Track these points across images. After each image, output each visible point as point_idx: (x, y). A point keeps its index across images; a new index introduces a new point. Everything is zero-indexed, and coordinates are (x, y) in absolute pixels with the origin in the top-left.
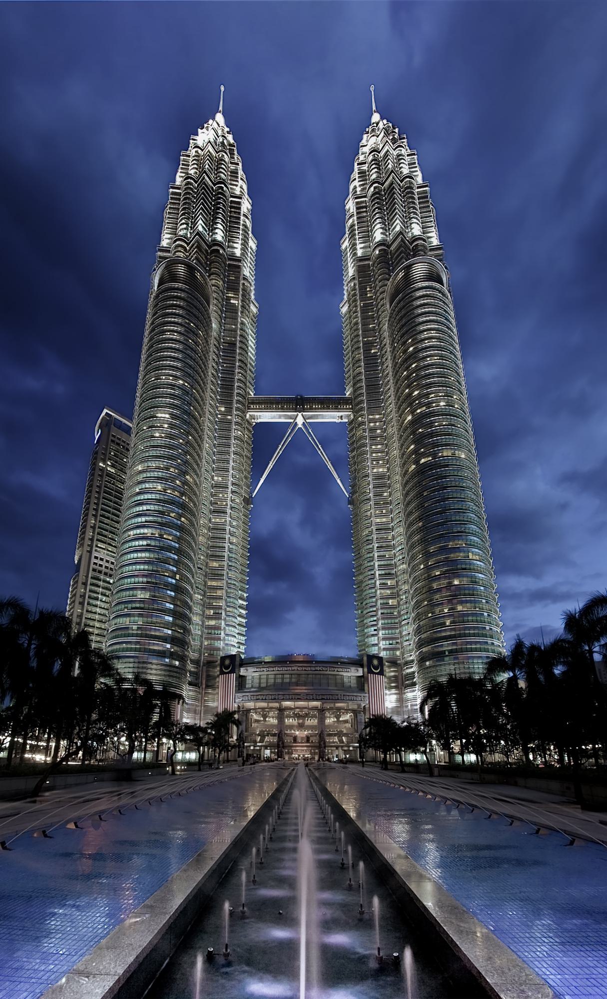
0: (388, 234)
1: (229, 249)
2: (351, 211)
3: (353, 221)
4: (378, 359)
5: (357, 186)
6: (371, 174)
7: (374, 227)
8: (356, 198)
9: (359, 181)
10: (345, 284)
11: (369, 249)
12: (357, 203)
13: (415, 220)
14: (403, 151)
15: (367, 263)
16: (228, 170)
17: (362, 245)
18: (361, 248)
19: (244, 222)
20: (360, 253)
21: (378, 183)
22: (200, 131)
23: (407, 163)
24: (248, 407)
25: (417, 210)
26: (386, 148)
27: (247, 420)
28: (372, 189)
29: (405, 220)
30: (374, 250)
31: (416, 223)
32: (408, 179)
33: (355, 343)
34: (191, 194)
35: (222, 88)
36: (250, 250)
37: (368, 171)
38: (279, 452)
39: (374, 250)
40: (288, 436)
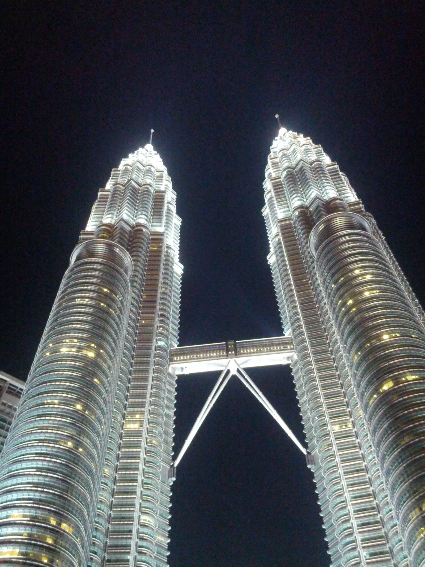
0: (305, 200)
1: (152, 228)
3: (271, 195)
4: (315, 304)
5: (272, 172)
6: (283, 163)
8: (271, 180)
11: (289, 212)
12: (273, 183)
14: (309, 147)
15: (288, 222)
16: (154, 177)
19: (168, 207)
23: (314, 153)
24: (169, 359)
25: (330, 181)
26: (294, 147)
27: (169, 374)
29: (320, 189)
30: (293, 212)
32: (317, 163)
33: (287, 286)
34: (119, 194)
36: (173, 225)
37: (280, 162)
39: (293, 212)
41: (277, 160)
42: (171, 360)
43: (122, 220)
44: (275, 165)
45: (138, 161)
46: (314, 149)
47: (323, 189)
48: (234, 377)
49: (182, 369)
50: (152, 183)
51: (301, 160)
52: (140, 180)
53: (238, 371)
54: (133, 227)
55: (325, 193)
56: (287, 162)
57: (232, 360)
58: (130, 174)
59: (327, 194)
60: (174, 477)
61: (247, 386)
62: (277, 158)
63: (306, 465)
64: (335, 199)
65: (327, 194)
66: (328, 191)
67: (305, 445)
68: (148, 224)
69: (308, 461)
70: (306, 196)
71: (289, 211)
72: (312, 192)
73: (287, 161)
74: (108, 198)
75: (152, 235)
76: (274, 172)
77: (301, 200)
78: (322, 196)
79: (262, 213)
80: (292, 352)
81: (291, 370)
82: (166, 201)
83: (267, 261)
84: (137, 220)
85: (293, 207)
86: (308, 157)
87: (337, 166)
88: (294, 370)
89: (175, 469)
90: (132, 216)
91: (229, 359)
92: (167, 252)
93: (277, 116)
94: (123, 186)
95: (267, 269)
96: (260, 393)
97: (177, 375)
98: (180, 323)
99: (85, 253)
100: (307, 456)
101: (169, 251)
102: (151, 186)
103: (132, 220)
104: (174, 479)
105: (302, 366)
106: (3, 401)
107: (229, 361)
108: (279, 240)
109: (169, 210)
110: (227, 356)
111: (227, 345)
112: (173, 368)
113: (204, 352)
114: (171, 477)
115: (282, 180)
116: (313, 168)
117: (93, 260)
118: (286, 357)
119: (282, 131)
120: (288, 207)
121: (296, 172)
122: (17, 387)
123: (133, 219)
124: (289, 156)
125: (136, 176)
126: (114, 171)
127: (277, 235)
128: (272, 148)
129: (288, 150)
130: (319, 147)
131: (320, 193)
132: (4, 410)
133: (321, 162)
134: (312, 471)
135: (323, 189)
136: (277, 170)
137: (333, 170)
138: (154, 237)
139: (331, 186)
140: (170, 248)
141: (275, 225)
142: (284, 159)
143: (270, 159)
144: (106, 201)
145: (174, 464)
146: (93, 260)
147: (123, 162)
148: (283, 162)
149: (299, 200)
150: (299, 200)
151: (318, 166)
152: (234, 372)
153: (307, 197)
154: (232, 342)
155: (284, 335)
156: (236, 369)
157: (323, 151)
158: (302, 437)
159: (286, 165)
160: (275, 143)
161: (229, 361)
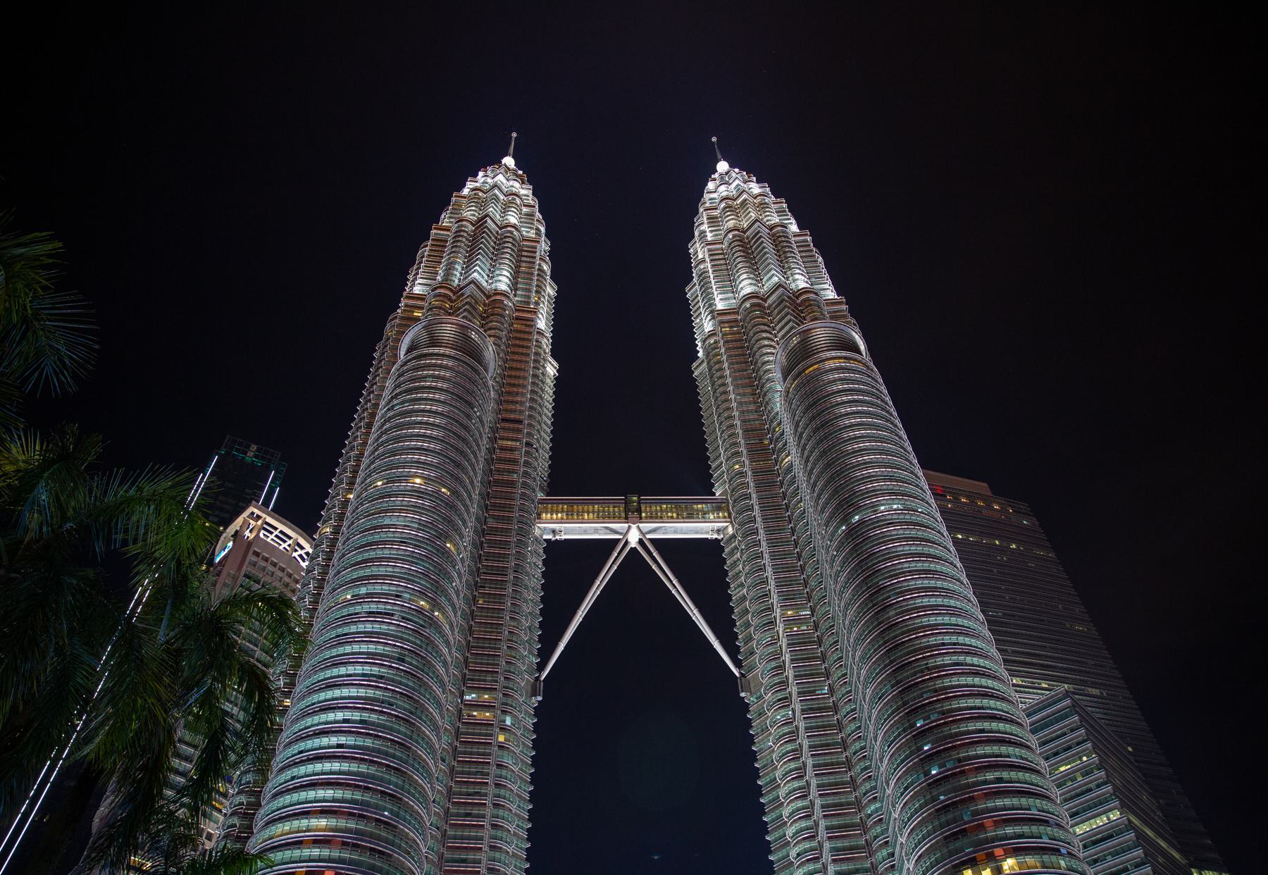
2: (700, 256)
7: (739, 277)
9: (709, 227)
10: (699, 344)
12: (709, 250)
13: (798, 271)
14: (767, 200)
17: (720, 297)
18: (721, 299)
20: (720, 306)
21: (738, 230)
22: (481, 174)
27: (536, 539)
28: (730, 236)
31: (799, 273)
35: (514, 135)
38: (595, 592)
40: (613, 563)
41: (716, 213)
43: (473, 282)
44: (713, 220)
45: (496, 186)
46: (774, 203)
47: (789, 273)
48: (633, 550)
50: (517, 223)
51: (757, 221)
52: (498, 217)
53: (641, 542)
54: (488, 297)
55: (791, 279)
56: (733, 219)
57: (634, 527)
58: (482, 206)
59: (794, 280)
61: (654, 567)
62: (716, 209)
63: (739, 694)
64: (805, 291)
65: (794, 280)
66: (797, 277)
67: (738, 664)
68: (510, 291)
70: (761, 280)
71: (735, 298)
72: (773, 275)
73: (733, 217)
74: (447, 241)
75: (517, 310)
76: (711, 231)
77: (755, 285)
78: (786, 283)
79: (687, 294)
80: (726, 522)
81: (722, 549)
82: (538, 258)
83: (693, 372)
84: (493, 286)
85: (741, 294)
86: (766, 216)
87: (809, 238)
88: (727, 550)
89: (542, 683)
90: (486, 277)
92: (537, 341)
93: (714, 139)
94: (473, 225)
95: (692, 384)
97: (545, 540)
98: (550, 457)
99: (424, 337)
100: (741, 680)
101: (540, 339)
102: (517, 229)
103: (486, 284)
104: (540, 698)
105: (743, 547)
106: (256, 549)
107: (629, 527)
108: (716, 342)
109: (541, 270)
110: (626, 518)
114: (535, 696)
115: (724, 246)
116: (773, 236)
117: (442, 351)
119: (723, 166)
120: (733, 292)
121: (748, 238)
122: (276, 529)
123: (487, 282)
124: (736, 209)
125: (494, 211)
126: (456, 196)
127: (712, 334)
128: (708, 193)
129: (735, 200)
130: (782, 203)
131: (783, 277)
132: (256, 563)
133: (786, 227)
135: (789, 273)
136: (715, 228)
137: (803, 244)
138: (521, 314)
139: (800, 269)
140: (543, 334)
141: (709, 317)
142: (729, 213)
143: (705, 210)
144: (445, 247)
145: (539, 677)
146: (436, 350)
147: (470, 185)
148: (727, 219)
149: (751, 284)
150: (751, 284)
151: (781, 234)
153: (764, 280)
154: (635, 498)
155: (714, 494)
156: (637, 540)
157: (787, 210)
158: (733, 651)
159: (731, 224)
160: (711, 185)
161: (629, 527)
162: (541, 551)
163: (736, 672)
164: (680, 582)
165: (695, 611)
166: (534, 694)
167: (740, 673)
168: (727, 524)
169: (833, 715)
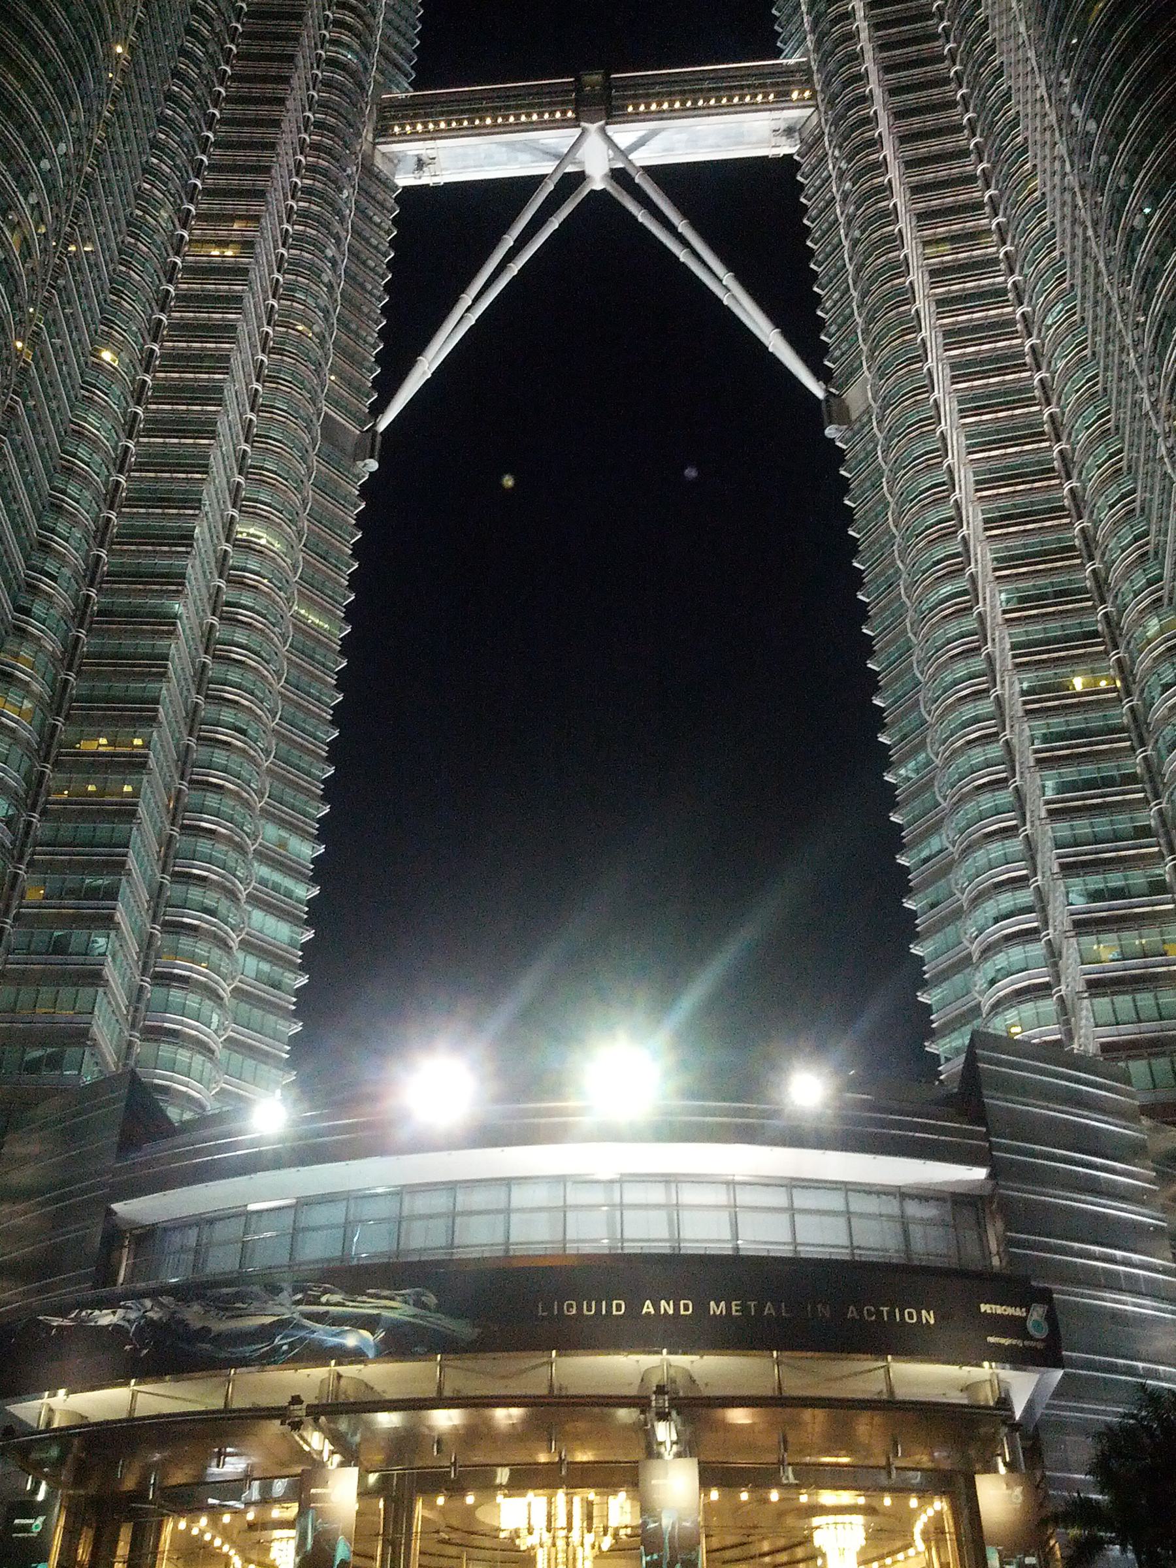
42: (383, 132)
49: (420, 164)
57: (593, 127)
60: (371, 457)
61: (641, 216)
69: (830, 416)
88: (806, 168)
89: (379, 438)
91: (583, 124)
96: (682, 226)
104: (373, 465)
111: (578, 86)
112: (388, 157)
113: (494, 111)
118: (783, 126)
134: (839, 444)
152: (598, 182)
154: (597, 78)
156: (605, 170)
158: (813, 354)
162: (391, 202)
163: (817, 390)
164: (695, 225)
165: (728, 278)
166: (360, 454)
167: (827, 391)
168: (812, 109)
169: (1050, 446)
